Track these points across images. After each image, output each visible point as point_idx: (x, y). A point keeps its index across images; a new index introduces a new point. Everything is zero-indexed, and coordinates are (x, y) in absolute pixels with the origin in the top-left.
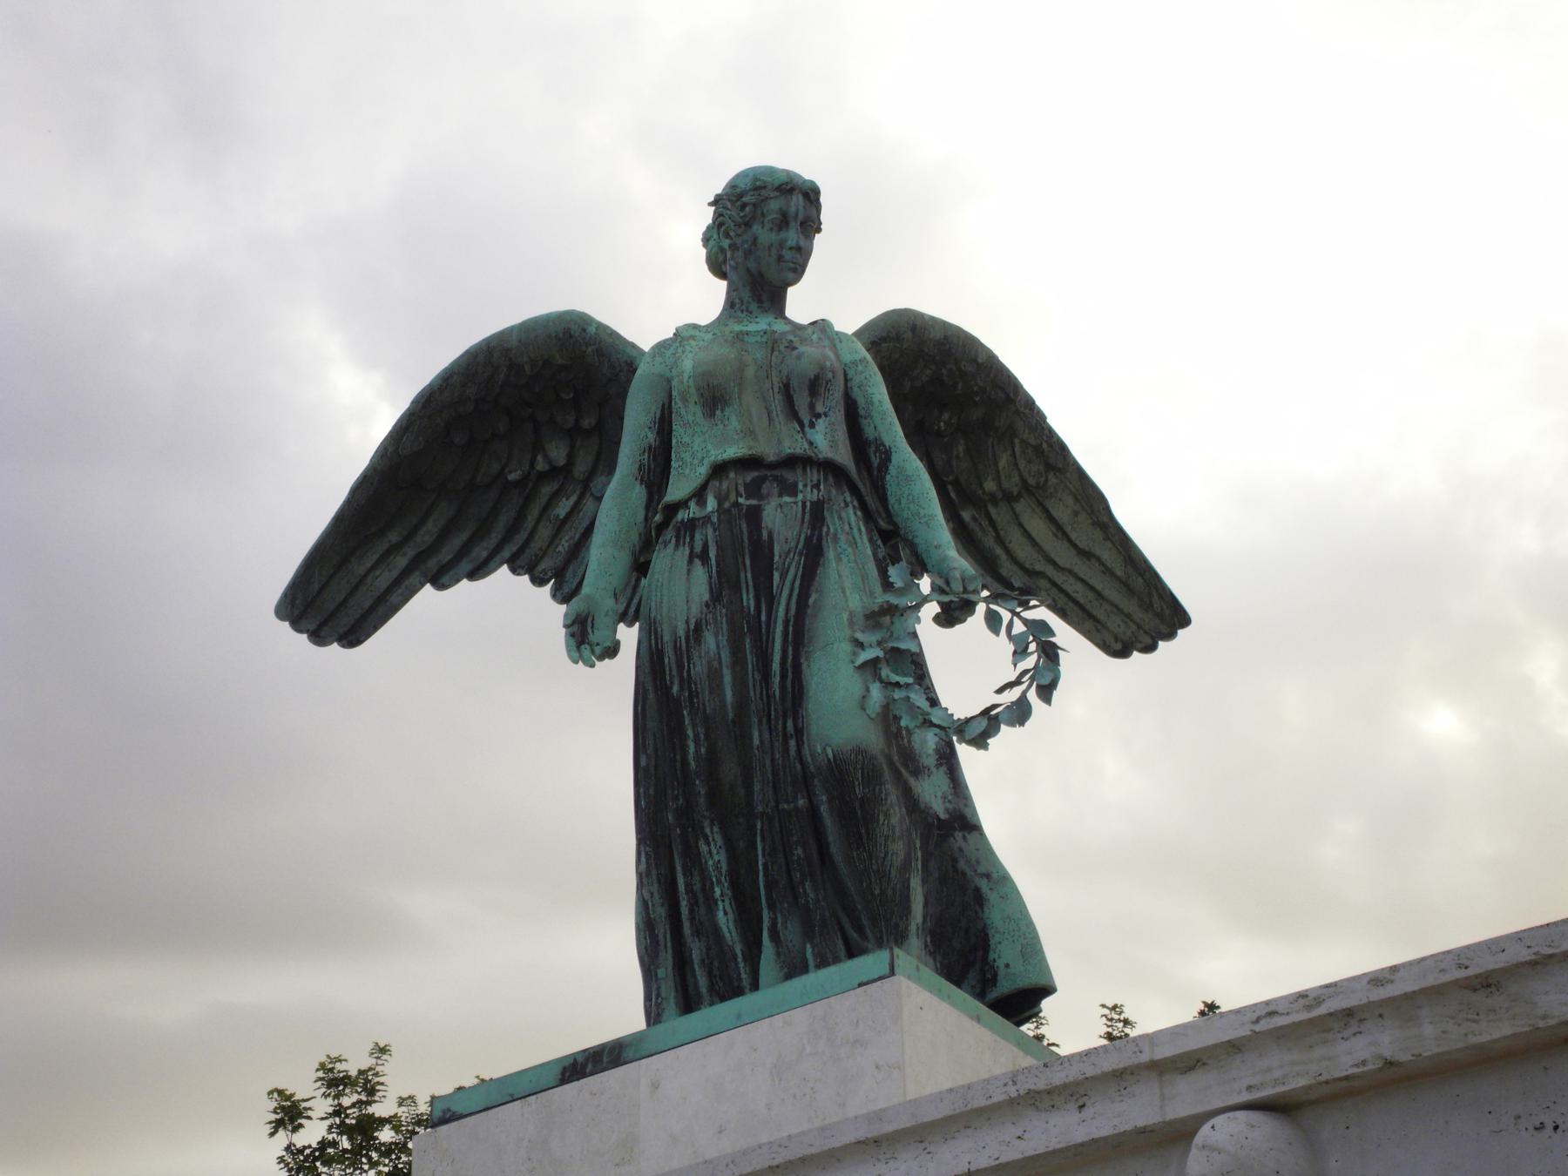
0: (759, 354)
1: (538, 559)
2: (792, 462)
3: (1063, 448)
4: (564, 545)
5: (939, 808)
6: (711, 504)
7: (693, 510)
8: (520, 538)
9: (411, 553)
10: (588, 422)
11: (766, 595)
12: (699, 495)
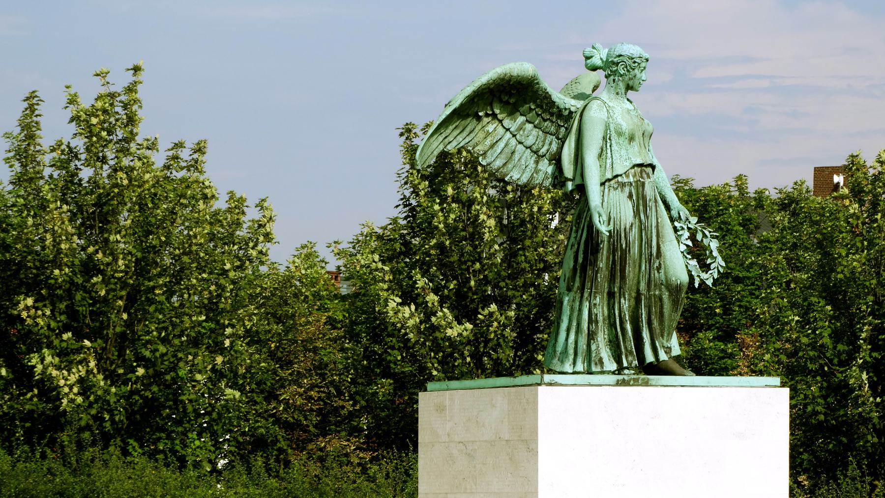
4: (488, 142)
8: (472, 135)
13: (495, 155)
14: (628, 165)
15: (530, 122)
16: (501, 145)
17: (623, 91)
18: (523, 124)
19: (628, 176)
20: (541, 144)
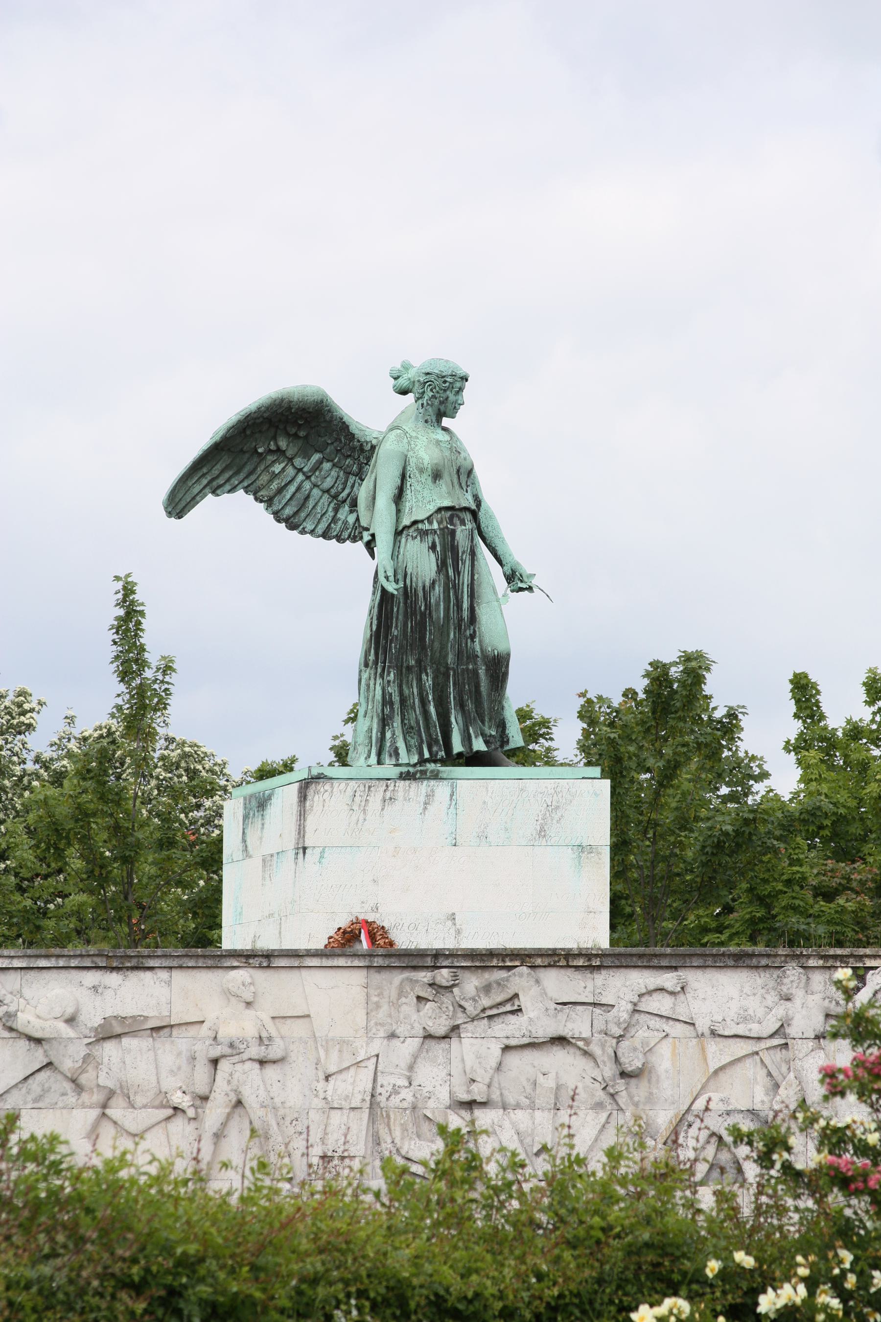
1: (260, 489)
4: (274, 486)
6: (435, 526)
7: (426, 526)
8: (253, 477)
9: (209, 478)
10: (302, 434)
11: (457, 572)
12: (429, 519)
13: (284, 501)
14: (432, 508)
15: (328, 461)
16: (292, 489)
17: (434, 419)
18: (320, 462)
19: (431, 523)
20: (341, 486)
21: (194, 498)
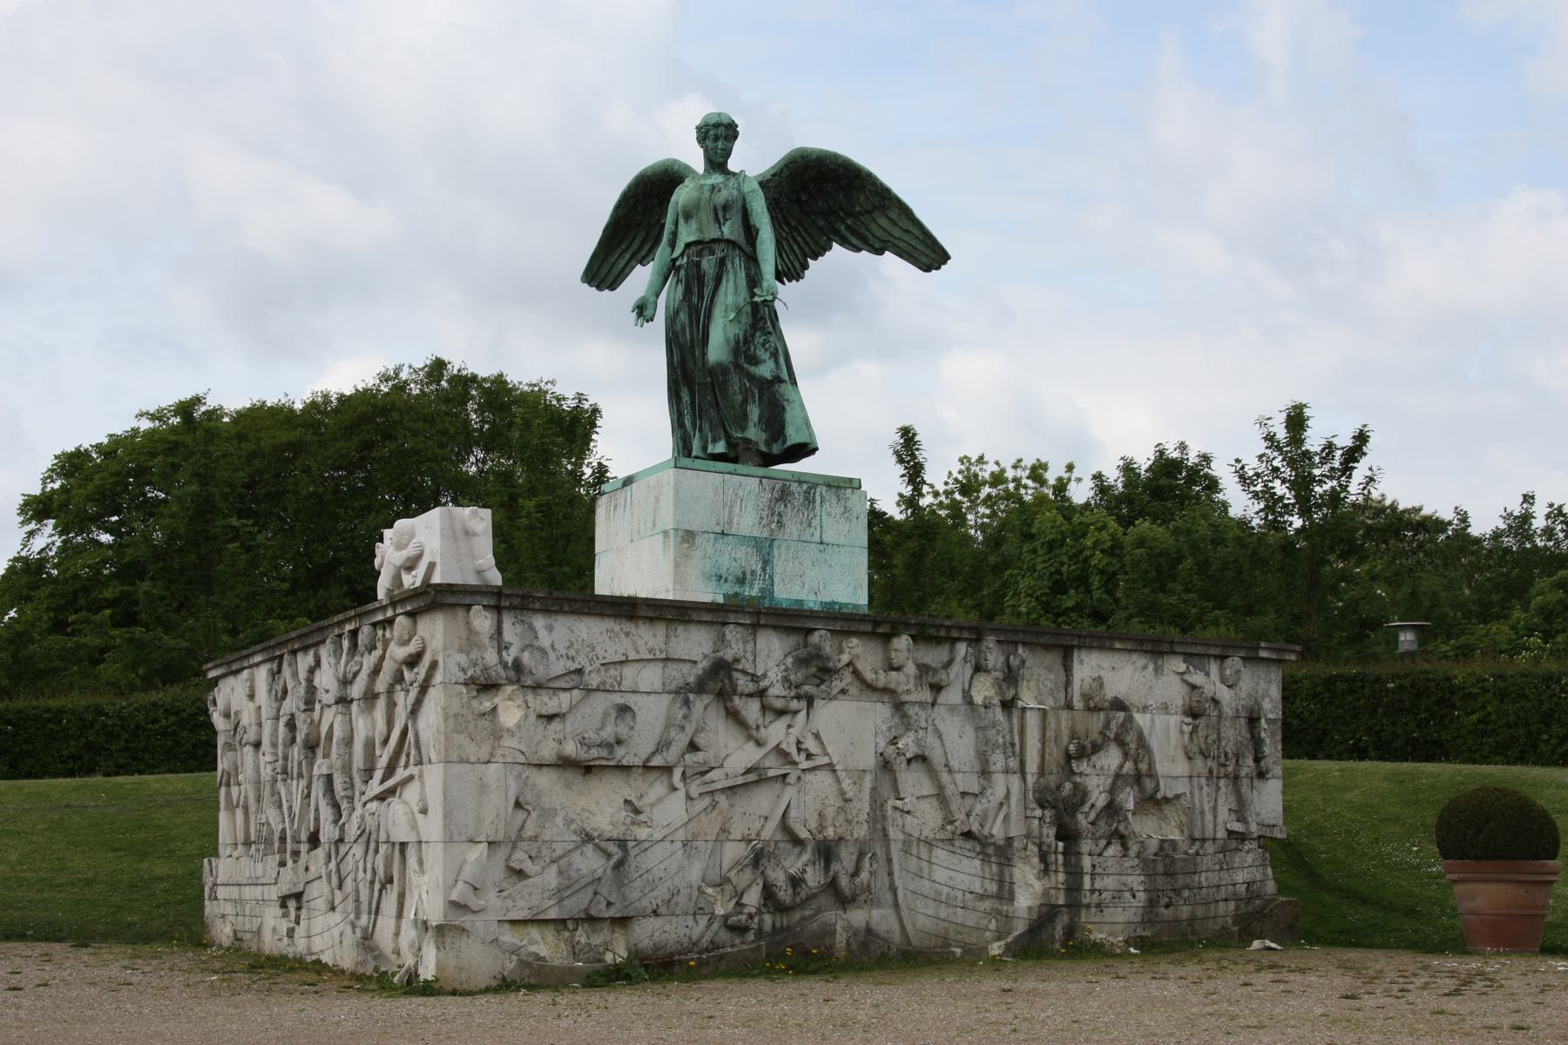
0: (707, 194)
2: (714, 241)
3: (888, 191)
5: (768, 376)
11: (701, 297)
12: (682, 255)
21: (622, 270)
